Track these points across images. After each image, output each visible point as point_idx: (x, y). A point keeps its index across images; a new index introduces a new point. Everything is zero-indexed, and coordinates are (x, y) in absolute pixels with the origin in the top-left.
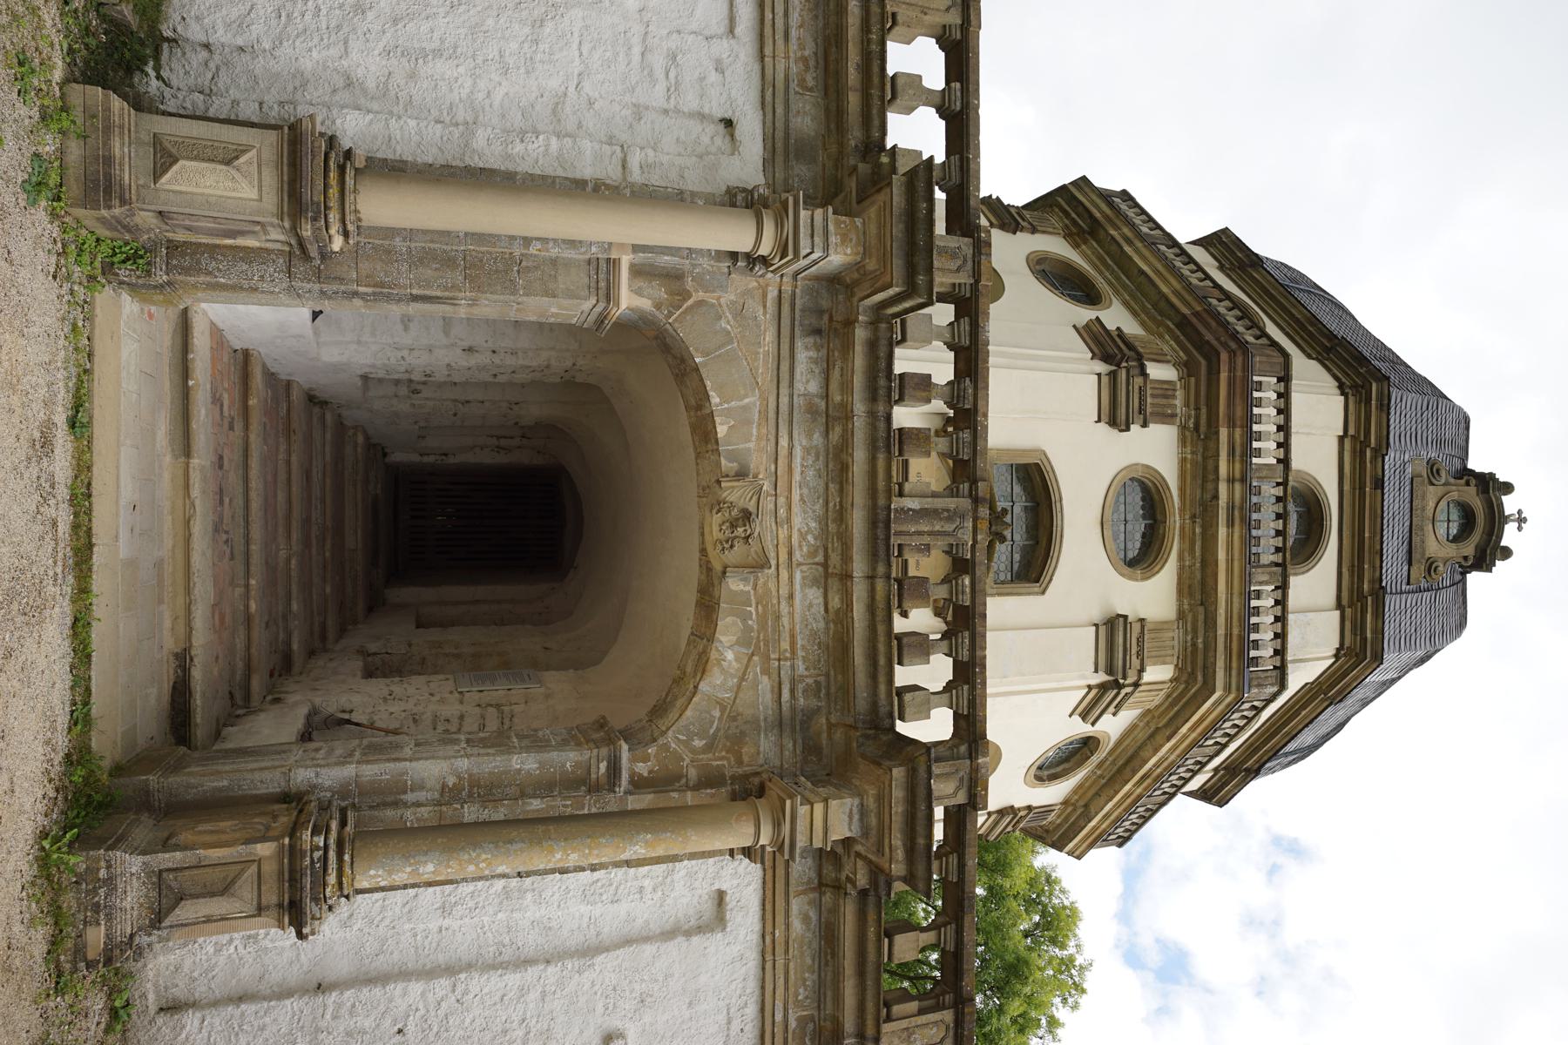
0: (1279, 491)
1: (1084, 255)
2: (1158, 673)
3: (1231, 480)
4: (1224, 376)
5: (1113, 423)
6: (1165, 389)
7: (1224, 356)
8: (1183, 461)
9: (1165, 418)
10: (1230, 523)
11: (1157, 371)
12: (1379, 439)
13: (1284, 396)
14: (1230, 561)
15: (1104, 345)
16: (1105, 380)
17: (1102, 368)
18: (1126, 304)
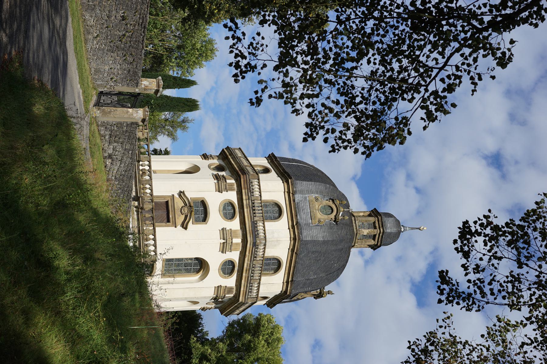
0: (260, 201)
1: (225, 163)
2: (238, 240)
3: (246, 200)
4: (242, 180)
5: (219, 192)
6: (231, 185)
7: (242, 176)
8: (238, 198)
9: (232, 190)
10: (247, 208)
11: (228, 181)
12: (292, 191)
13: (259, 182)
14: (248, 216)
15: (217, 177)
16: (217, 184)
17: (216, 181)
18: (230, 171)
